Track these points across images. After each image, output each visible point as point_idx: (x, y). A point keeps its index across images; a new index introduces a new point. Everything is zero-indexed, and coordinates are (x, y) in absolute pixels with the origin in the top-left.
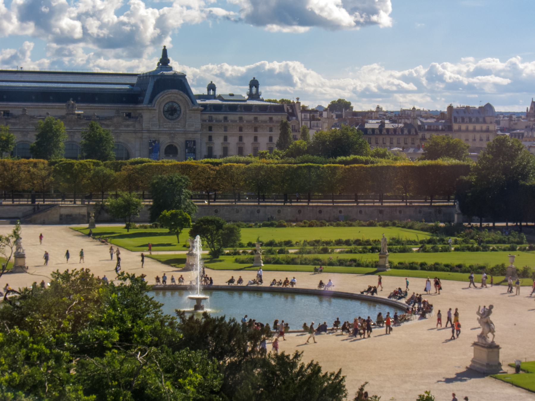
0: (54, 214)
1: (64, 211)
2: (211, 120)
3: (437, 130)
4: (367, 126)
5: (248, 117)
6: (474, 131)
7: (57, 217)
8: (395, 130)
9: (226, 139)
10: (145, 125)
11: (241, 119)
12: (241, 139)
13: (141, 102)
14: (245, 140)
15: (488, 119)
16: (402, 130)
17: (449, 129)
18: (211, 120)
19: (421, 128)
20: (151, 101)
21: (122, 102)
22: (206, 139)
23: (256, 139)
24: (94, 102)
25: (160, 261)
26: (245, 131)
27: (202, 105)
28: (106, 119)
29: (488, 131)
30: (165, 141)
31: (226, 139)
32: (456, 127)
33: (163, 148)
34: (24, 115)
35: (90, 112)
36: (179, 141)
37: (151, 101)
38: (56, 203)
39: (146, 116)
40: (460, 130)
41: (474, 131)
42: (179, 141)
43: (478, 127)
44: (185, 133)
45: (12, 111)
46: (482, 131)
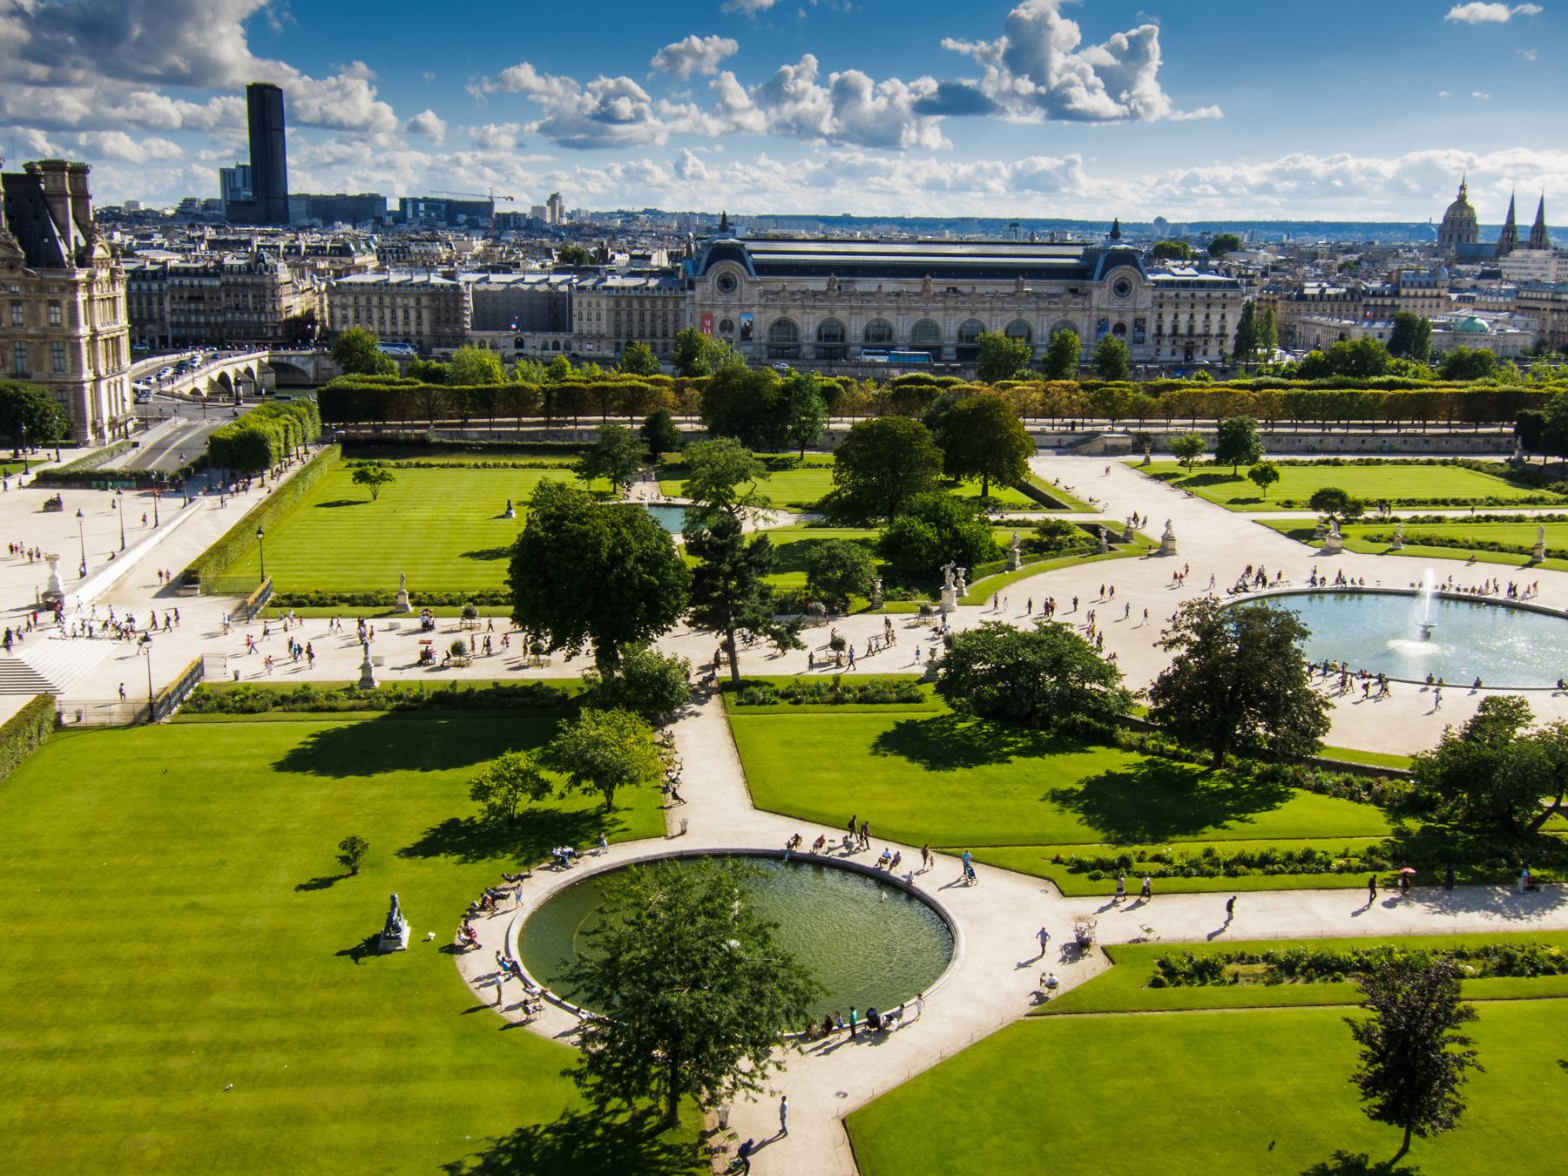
0: (1098, 445)
1: (1109, 442)
2: (1162, 296)
3: (1382, 295)
4: (1306, 291)
5: (1201, 293)
6: (1424, 296)
7: (1100, 448)
8: (1337, 296)
9: (1176, 316)
10: (1094, 303)
11: (1193, 296)
12: (1192, 316)
13: (1091, 278)
14: (1197, 317)
15: (1440, 284)
16: (1345, 295)
17: (1397, 294)
18: (1162, 296)
19: (1365, 293)
20: (1101, 278)
21: (1069, 277)
22: (1156, 317)
23: (1207, 316)
24: (1042, 278)
25: (1278, 531)
26: (1197, 308)
27: (1155, 281)
28: (1054, 295)
29: (1438, 296)
30: (1114, 319)
31: (1176, 316)
32: (1403, 292)
33: (1111, 327)
34: (973, 292)
35: (1039, 289)
36: (1128, 320)
37: (1101, 278)
38: (1098, 428)
39: (1096, 293)
40: (1407, 296)
41: (1416, 296)
42: (1128, 320)
43: (1428, 292)
44: (1135, 310)
45: (960, 288)
46: (1432, 297)
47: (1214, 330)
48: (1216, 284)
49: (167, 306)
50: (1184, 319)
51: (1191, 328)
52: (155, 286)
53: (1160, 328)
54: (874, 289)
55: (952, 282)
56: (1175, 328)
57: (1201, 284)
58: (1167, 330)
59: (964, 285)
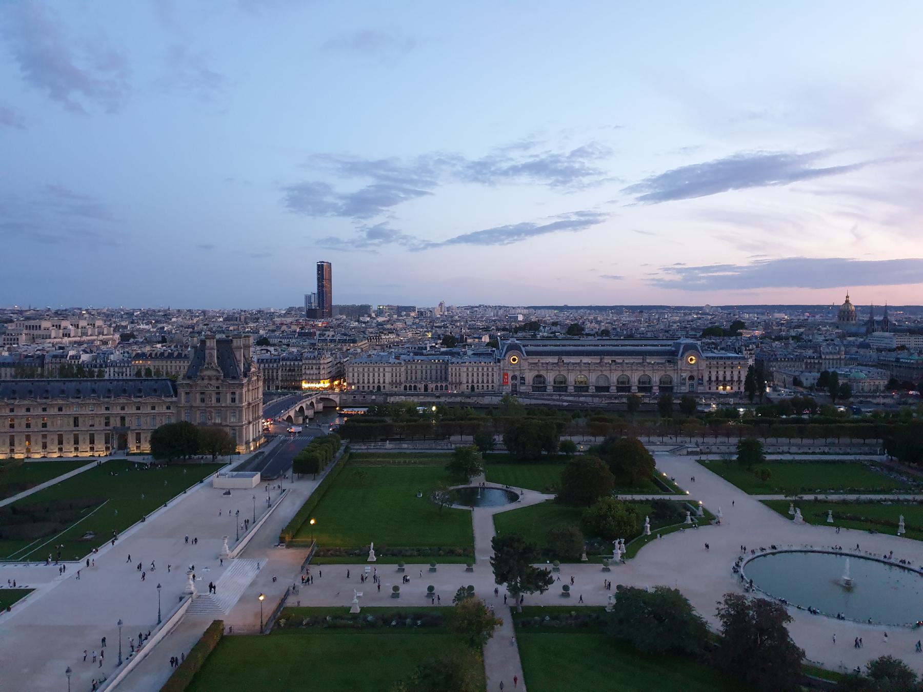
47: (736, 378)
48: (736, 358)
49: (280, 373)
50: (721, 373)
51: (725, 378)
52: (275, 365)
53: (710, 378)
54: (579, 361)
55: (614, 358)
56: (717, 378)
57: (729, 358)
58: (713, 378)
59: (619, 360)
